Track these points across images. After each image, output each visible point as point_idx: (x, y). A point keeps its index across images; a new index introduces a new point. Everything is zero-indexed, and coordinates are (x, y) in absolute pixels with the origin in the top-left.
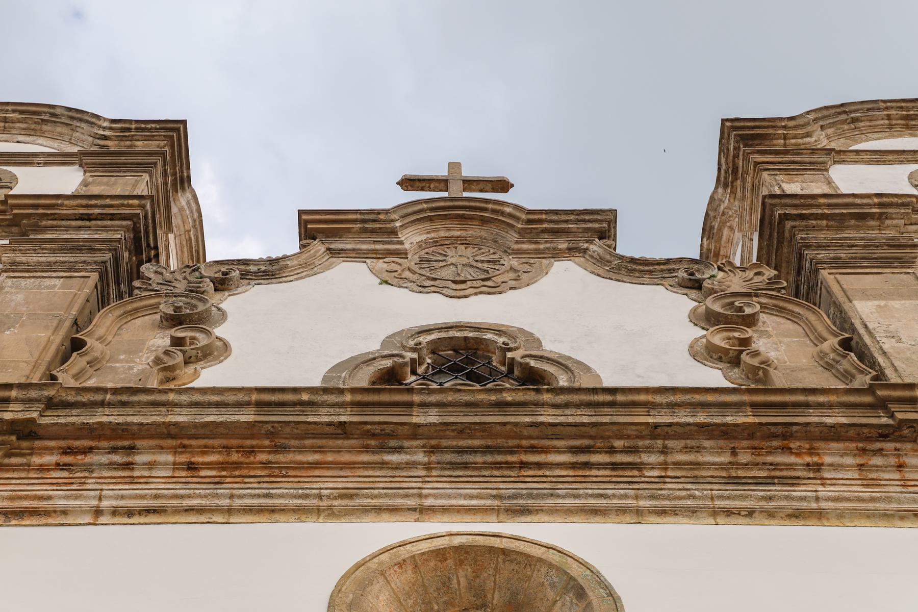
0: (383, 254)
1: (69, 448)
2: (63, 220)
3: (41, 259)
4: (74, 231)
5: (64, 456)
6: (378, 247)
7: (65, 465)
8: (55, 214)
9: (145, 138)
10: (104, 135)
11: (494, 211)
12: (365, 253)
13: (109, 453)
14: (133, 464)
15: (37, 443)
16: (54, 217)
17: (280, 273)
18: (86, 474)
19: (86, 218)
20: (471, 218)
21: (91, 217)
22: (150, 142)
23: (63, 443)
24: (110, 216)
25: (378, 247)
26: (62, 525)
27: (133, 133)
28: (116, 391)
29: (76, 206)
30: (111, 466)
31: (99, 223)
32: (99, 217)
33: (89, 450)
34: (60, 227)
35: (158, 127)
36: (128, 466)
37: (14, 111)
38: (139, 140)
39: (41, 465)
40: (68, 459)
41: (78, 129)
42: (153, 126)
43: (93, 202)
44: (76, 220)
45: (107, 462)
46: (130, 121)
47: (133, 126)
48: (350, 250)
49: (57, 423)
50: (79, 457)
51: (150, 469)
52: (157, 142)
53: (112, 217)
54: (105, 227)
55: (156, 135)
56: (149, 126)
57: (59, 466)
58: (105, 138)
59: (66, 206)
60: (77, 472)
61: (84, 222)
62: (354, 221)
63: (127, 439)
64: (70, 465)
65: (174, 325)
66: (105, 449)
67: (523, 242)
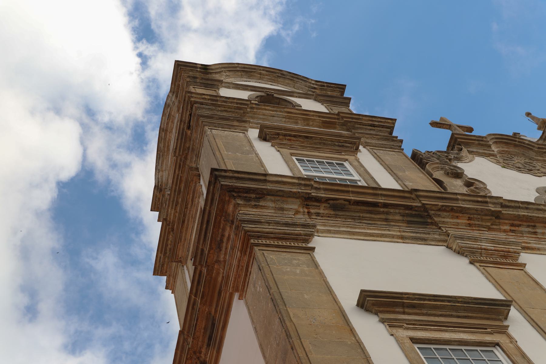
0: (488, 155)
1: (513, 224)
2: (364, 125)
3: (376, 142)
4: (369, 131)
5: (511, 227)
6: (486, 152)
7: (513, 230)
8: (361, 122)
9: (331, 91)
10: (314, 87)
11: (519, 142)
12: (481, 154)
13: (527, 227)
14: (536, 232)
15: (501, 221)
16: (361, 124)
17: (461, 159)
18: (522, 235)
19: (373, 125)
20: (510, 144)
21: (375, 126)
22: (334, 93)
23: (511, 222)
24: (382, 126)
25: (486, 152)
26: (541, 254)
27: (326, 88)
28: (522, 203)
29: (368, 120)
30: (529, 232)
31: (378, 128)
32: (378, 126)
33: (519, 226)
34: (363, 128)
35: (336, 86)
36: (535, 233)
37: (263, 70)
38: (328, 91)
39: (505, 230)
40: (513, 228)
41: (297, 82)
42: (334, 86)
43: (374, 119)
44: (369, 126)
45: (528, 231)
46: (324, 82)
47: (325, 85)
48: (475, 152)
49: (509, 213)
50: (516, 228)
51: (543, 235)
52: (337, 93)
53: (383, 127)
54: (380, 130)
55: (336, 90)
56: (332, 85)
57: (511, 231)
58: (315, 88)
59: (364, 120)
60: (518, 234)
61: (372, 127)
62: (475, 140)
63: (531, 222)
64: (515, 231)
65: (455, 177)
66: (525, 226)
67: (538, 156)
